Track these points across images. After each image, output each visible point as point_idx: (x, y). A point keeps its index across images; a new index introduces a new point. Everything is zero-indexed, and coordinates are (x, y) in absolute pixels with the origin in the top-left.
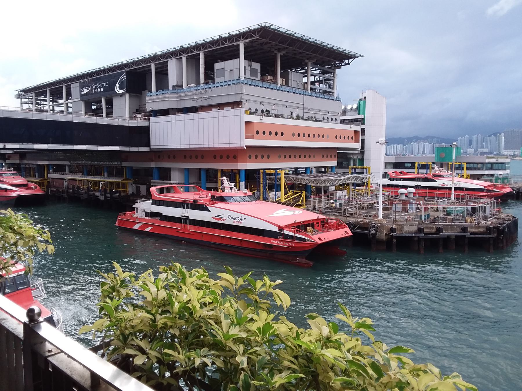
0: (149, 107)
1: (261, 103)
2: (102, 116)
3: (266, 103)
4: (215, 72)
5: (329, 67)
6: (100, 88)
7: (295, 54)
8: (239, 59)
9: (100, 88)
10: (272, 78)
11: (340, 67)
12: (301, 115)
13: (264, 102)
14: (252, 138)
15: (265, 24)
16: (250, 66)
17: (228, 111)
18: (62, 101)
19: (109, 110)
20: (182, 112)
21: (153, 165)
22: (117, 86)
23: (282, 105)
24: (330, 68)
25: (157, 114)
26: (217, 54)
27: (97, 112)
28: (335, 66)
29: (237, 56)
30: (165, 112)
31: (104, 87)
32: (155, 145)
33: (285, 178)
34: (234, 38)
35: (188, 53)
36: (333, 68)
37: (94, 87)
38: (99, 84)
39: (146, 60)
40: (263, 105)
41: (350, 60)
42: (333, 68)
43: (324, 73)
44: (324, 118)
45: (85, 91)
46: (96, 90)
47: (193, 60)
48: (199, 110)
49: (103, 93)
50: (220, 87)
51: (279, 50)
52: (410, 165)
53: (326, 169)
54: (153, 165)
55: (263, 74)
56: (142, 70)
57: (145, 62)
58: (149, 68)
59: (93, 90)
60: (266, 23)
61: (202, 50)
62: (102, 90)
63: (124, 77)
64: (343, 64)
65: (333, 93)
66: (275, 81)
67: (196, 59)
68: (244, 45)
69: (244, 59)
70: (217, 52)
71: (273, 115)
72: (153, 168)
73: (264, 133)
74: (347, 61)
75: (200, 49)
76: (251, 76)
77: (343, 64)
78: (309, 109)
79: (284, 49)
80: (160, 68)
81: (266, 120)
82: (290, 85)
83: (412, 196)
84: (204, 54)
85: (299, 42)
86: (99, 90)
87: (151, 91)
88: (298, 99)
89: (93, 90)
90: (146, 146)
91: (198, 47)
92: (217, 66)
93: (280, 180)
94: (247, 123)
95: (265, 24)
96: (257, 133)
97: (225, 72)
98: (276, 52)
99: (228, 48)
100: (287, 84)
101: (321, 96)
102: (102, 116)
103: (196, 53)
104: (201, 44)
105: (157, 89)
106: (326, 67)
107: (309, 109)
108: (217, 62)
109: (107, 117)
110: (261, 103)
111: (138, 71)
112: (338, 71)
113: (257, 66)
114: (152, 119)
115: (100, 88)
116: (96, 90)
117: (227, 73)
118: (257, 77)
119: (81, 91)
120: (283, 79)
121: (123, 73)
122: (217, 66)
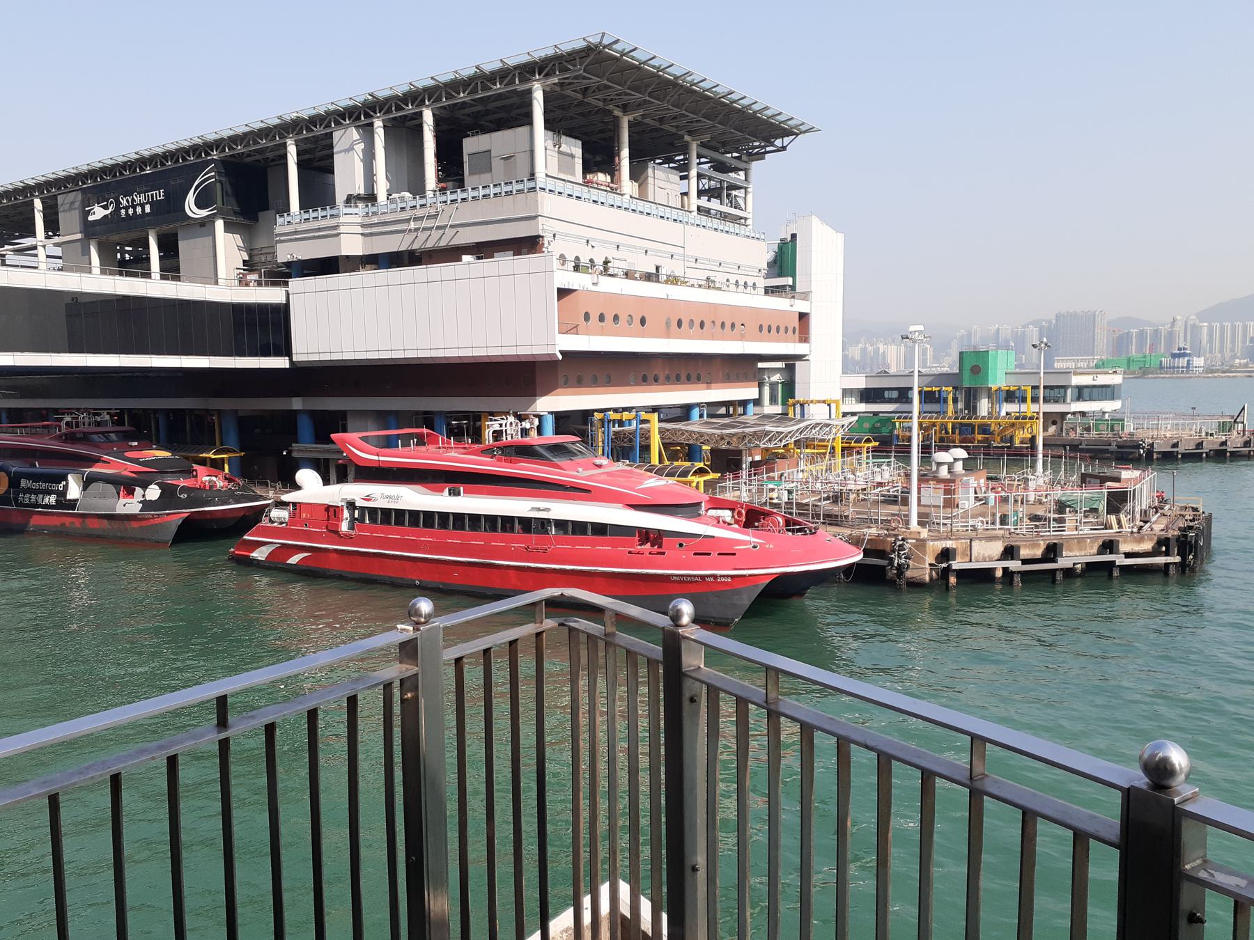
0: (285, 253)
1: (588, 241)
2: (148, 276)
4: (466, 158)
5: (735, 155)
6: (142, 205)
7: (661, 120)
8: (524, 130)
9: (141, 202)
10: (609, 178)
11: (760, 156)
13: (595, 240)
14: (573, 330)
15: (602, 37)
16: (557, 144)
17: (504, 263)
18: (28, 242)
20: (374, 266)
21: (297, 404)
22: (191, 198)
23: (634, 247)
25: (305, 272)
27: (137, 265)
28: (750, 154)
29: (528, 120)
30: (328, 266)
31: (152, 204)
32: (306, 352)
33: (660, 432)
35: (389, 111)
36: (744, 158)
37: (124, 203)
38: (139, 193)
39: (271, 132)
40: (593, 247)
41: (787, 140)
42: (744, 158)
43: (721, 167)
44: (728, 280)
45: (98, 213)
46: (131, 211)
48: (423, 261)
51: (625, 108)
52: (895, 394)
53: (731, 409)
54: (297, 404)
55: (587, 168)
56: (258, 157)
57: (267, 135)
58: (281, 152)
59: (123, 211)
61: (427, 103)
63: (208, 176)
64: (768, 149)
65: (746, 219)
66: (614, 190)
68: (544, 91)
69: (545, 128)
70: (463, 111)
73: (602, 318)
74: (778, 143)
76: (560, 170)
78: (696, 260)
79: (638, 106)
81: (608, 285)
85: (677, 89)
86: (139, 210)
87: (286, 209)
89: (123, 211)
90: (278, 354)
91: (416, 97)
92: (471, 145)
93: (648, 438)
94: (563, 293)
95: (602, 37)
96: (587, 317)
97: (493, 160)
98: (617, 113)
100: (643, 196)
101: (721, 227)
102: (148, 276)
103: (410, 109)
104: (425, 90)
105: (304, 206)
106: (729, 155)
107: (696, 260)
108: (468, 136)
109: (163, 277)
110: (588, 241)
112: (755, 166)
113: (574, 148)
114: (296, 284)
115: (142, 205)
116: (131, 211)
117: (497, 164)
118: (573, 174)
120: (635, 183)
121: (207, 163)
122: (471, 145)
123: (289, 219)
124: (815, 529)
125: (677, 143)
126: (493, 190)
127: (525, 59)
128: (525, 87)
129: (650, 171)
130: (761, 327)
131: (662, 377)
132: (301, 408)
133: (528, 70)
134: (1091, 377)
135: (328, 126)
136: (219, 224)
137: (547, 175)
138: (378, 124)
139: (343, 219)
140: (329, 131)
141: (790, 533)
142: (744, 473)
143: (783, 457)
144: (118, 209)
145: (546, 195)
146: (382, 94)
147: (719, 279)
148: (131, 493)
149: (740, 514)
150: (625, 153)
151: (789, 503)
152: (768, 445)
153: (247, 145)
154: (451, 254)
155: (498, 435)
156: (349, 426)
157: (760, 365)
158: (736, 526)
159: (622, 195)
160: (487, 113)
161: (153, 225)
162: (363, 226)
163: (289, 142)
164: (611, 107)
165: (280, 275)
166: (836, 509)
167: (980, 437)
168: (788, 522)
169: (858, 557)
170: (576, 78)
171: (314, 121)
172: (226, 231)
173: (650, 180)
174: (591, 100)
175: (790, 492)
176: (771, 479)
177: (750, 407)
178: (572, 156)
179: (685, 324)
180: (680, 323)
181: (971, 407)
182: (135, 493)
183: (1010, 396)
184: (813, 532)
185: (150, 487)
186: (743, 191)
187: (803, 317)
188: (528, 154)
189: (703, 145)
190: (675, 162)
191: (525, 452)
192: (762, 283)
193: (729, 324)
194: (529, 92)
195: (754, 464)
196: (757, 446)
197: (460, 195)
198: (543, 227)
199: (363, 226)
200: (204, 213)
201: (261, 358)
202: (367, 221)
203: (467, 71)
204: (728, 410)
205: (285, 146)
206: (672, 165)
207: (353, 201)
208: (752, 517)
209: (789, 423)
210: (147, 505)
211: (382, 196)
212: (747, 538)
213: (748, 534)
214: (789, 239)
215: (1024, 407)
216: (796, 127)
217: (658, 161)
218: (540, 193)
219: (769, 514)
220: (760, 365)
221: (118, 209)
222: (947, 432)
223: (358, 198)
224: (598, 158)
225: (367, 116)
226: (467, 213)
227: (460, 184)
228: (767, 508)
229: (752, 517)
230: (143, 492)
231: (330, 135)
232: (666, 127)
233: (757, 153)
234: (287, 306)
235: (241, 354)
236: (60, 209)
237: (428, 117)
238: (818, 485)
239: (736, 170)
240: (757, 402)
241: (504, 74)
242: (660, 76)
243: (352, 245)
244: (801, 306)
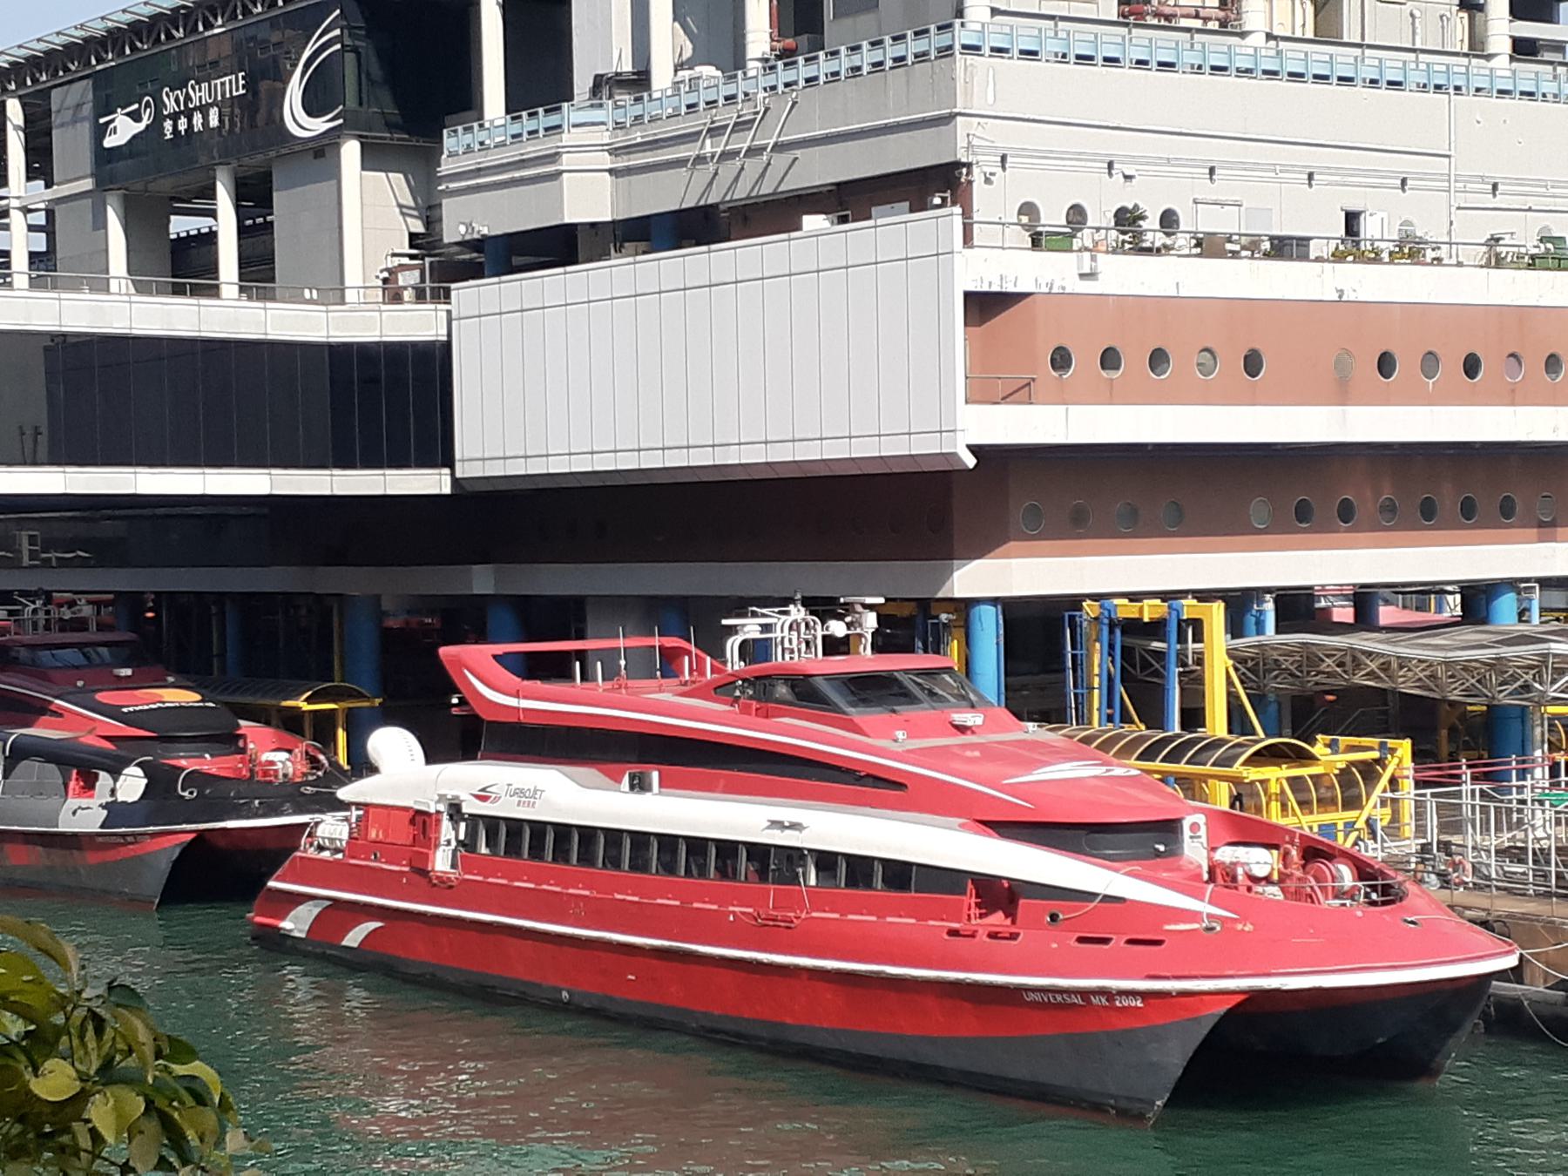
20: (642, 245)
82: (1351, 33)
114: (465, 293)
132: (491, 592)
139: (567, 138)
148: (89, 784)
156: (589, 632)
162: (615, 152)
182: (98, 784)
185: (126, 771)
199: (615, 152)
201: (388, 472)
202: (621, 139)
207: (605, 91)
210: (116, 812)
211: (662, 76)
230: (111, 782)
234: (447, 346)
235: (344, 460)
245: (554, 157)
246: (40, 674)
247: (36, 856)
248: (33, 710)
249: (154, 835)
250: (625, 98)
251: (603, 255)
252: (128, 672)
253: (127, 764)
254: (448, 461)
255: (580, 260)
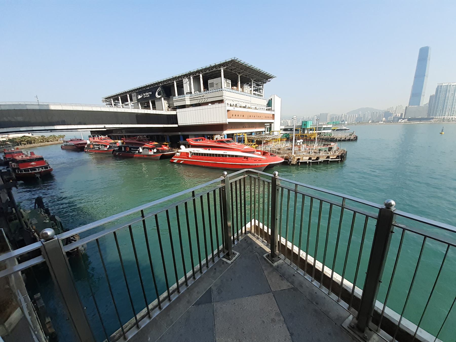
0: (176, 104)
3: (235, 100)
4: (209, 84)
5: (261, 82)
6: (148, 95)
7: (246, 75)
8: (220, 78)
9: (147, 95)
10: (236, 88)
11: (265, 83)
12: (250, 106)
13: (234, 100)
14: (230, 118)
16: (226, 81)
17: (217, 105)
18: (127, 103)
19: (153, 107)
22: (157, 93)
24: (261, 83)
26: (209, 75)
27: (148, 107)
28: (263, 82)
29: (220, 76)
30: (184, 107)
31: (150, 95)
34: (218, 66)
35: (193, 75)
36: (262, 83)
37: (144, 95)
40: (233, 102)
41: (270, 79)
42: (262, 83)
45: (140, 97)
47: (197, 79)
49: (149, 98)
50: (212, 93)
51: (239, 73)
55: (232, 86)
58: (173, 84)
59: (144, 97)
60: (235, 57)
61: (201, 73)
62: (149, 96)
64: (267, 81)
65: (262, 95)
66: (237, 90)
67: (197, 78)
71: (239, 107)
72: (180, 135)
74: (269, 80)
75: (200, 72)
77: (267, 81)
80: (178, 83)
82: (244, 92)
83: (301, 143)
84: (202, 76)
87: (175, 95)
88: (248, 98)
91: (198, 72)
92: (210, 81)
94: (228, 111)
97: (214, 85)
98: (237, 74)
99: (214, 72)
100: (243, 91)
102: (150, 109)
103: (197, 74)
105: (178, 95)
106: (259, 83)
108: (209, 80)
109: (153, 109)
111: (167, 85)
112: (264, 85)
114: (178, 110)
115: (148, 95)
116: (146, 96)
118: (229, 87)
119: (137, 97)
122: (210, 81)
123: (176, 97)
124: (276, 155)
125: (249, 80)
126: (214, 91)
127: (220, 63)
128: (220, 69)
129: (244, 86)
130: (265, 117)
131: (247, 127)
133: (220, 65)
134: (326, 126)
135: (182, 78)
136: (163, 99)
137: (224, 87)
138: (191, 77)
139: (186, 97)
140: (182, 79)
141: (271, 156)
142: (262, 145)
143: (269, 142)
144: (143, 96)
145: (224, 91)
146: (192, 71)
147: (258, 107)
149: (262, 153)
150: (239, 82)
151: (271, 150)
152: (267, 140)
153: (167, 82)
154: (207, 104)
155: (217, 139)
156: (189, 137)
157: (265, 124)
158: (261, 155)
159: (239, 91)
160: (213, 74)
161: (150, 99)
162: (190, 99)
163: (175, 82)
164: (236, 73)
165: (175, 109)
166: (279, 151)
167: (305, 137)
168: (271, 154)
169: (283, 160)
170: (230, 67)
171: (179, 77)
172: (164, 100)
173: (244, 88)
174: (232, 72)
175: (271, 148)
176: (267, 146)
177: (263, 132)
178: (229, 83)
179: (251, 116)
180: (250, 116)
181: (304, 132)
183: (311, 130)
184: (275, 156)
186: (262, 90)
187: (273, 115)
188: (221, 83)
189: (254, 81)
190: (249, 84)
191: (222, 142)
192: (266, 108)
193: (259, 117)
194: (220, 70)
195: (264, 143)
196: (265, 140)
197: (208, 92)
198: (224, 98)
199: (190, 99)
200: (160, 96)
202: (190, 98)
203: (208, 66)
204: (260, 133)
205: (174, 82)
206: (248, 85)
207: (188, 93)
208: (264, 154)
209: (270, 135)
211: (193, 93)
212: (264, 158)
213: (263, 157)
214: (270, 99)
215: (313, 132)
216: (272, 76)
217: (246, 84)
218: (223, 91)
219: (268, 153)
220: (265, 124)
221: (143, 96)
222: (299, 137)
223: (189, 93)
224: (234, 84)
225: (189, 76)
226: (209, 95)
227: (208, 90)
228: (267, 151)
229: (264, 154)
231: (182, 80)
232: (247, 77)
233: (265, 82)
234: (176, 115)
236: (132, 96)
237: (201, 76)
238: (276, 147)
239: (261, 86)
240: (265, 131)
241: (215, 66)
242: (246, 66)
243: (188, 102)
244: (273, 113)
245: (185, 99)
246: (144, 142)
247: (147, 156)
248: (144, 145)
249: (158, 154)
250: (189, 94)
251: (189, 107)
252: (151, 141)
253: (155, 149)
254: (177, 124)
255: (186, 107)
